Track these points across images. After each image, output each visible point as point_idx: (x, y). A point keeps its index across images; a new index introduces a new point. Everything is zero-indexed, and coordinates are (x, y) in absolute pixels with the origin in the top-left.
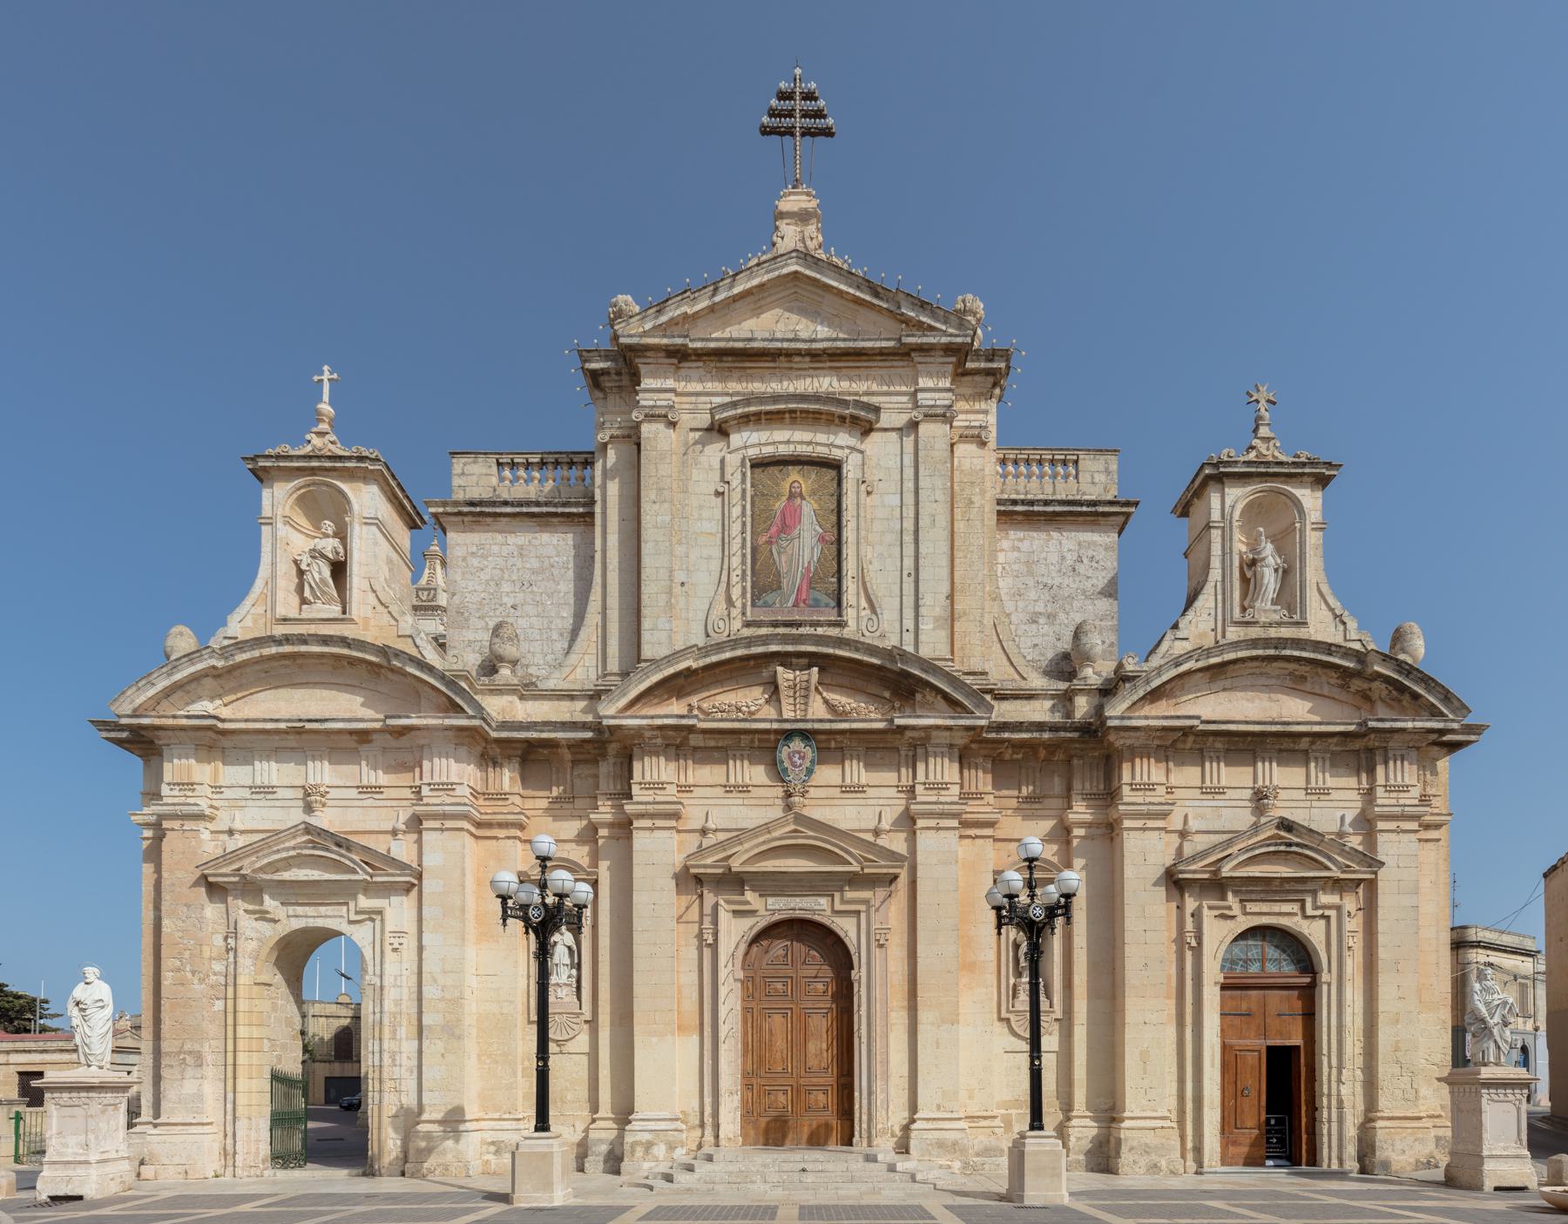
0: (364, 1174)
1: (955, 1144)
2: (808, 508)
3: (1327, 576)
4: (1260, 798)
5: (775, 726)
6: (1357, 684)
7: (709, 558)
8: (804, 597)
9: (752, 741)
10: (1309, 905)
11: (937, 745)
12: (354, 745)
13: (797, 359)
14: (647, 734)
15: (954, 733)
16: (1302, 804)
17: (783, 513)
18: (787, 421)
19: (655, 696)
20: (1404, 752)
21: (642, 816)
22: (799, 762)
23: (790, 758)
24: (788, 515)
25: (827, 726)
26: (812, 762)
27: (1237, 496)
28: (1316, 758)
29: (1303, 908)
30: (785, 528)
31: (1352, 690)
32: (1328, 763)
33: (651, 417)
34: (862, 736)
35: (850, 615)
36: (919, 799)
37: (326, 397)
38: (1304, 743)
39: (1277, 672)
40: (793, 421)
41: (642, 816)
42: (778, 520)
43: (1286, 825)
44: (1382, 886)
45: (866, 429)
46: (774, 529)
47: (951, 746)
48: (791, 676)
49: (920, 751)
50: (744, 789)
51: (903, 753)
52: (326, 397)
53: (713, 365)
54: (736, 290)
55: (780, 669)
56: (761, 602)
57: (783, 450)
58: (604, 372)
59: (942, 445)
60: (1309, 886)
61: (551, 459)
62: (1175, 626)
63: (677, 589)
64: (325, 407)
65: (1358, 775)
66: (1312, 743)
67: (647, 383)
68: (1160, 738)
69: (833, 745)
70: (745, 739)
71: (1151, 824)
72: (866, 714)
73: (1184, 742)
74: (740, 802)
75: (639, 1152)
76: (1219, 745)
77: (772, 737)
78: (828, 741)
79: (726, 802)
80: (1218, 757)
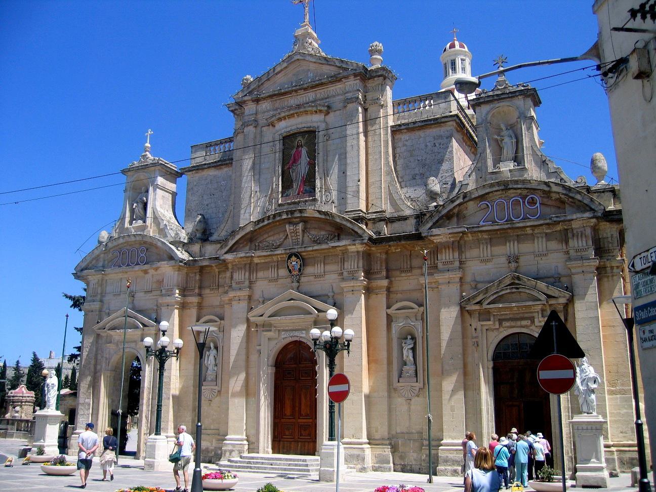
0: (135, 459)
1: (358, 456)
2: (304, 151)
8: (302, 190)
10: (536, 320)
11: (353, 252)
12: (143, 274)
13: (299, 91)
18: (296, 116)
19: (241, 244)
26: (301, 266)
28: (538, 237)
29: (533, 322)
30: (295, 161)
31: (553, 198)
32: (544, 239)
40: (298, 116)
45: (327, 113)
46: (291, 162)
47: (358, 252)
48: (292, 228)
50: (276, 280)
53: (270, 100)
55: (287, 226)
56: (285, 194)
58: (235, 110)
64: (148, 145)
73: (468, 237)
75: (228, 454)
76: (486, 237)
80: (486, 243)
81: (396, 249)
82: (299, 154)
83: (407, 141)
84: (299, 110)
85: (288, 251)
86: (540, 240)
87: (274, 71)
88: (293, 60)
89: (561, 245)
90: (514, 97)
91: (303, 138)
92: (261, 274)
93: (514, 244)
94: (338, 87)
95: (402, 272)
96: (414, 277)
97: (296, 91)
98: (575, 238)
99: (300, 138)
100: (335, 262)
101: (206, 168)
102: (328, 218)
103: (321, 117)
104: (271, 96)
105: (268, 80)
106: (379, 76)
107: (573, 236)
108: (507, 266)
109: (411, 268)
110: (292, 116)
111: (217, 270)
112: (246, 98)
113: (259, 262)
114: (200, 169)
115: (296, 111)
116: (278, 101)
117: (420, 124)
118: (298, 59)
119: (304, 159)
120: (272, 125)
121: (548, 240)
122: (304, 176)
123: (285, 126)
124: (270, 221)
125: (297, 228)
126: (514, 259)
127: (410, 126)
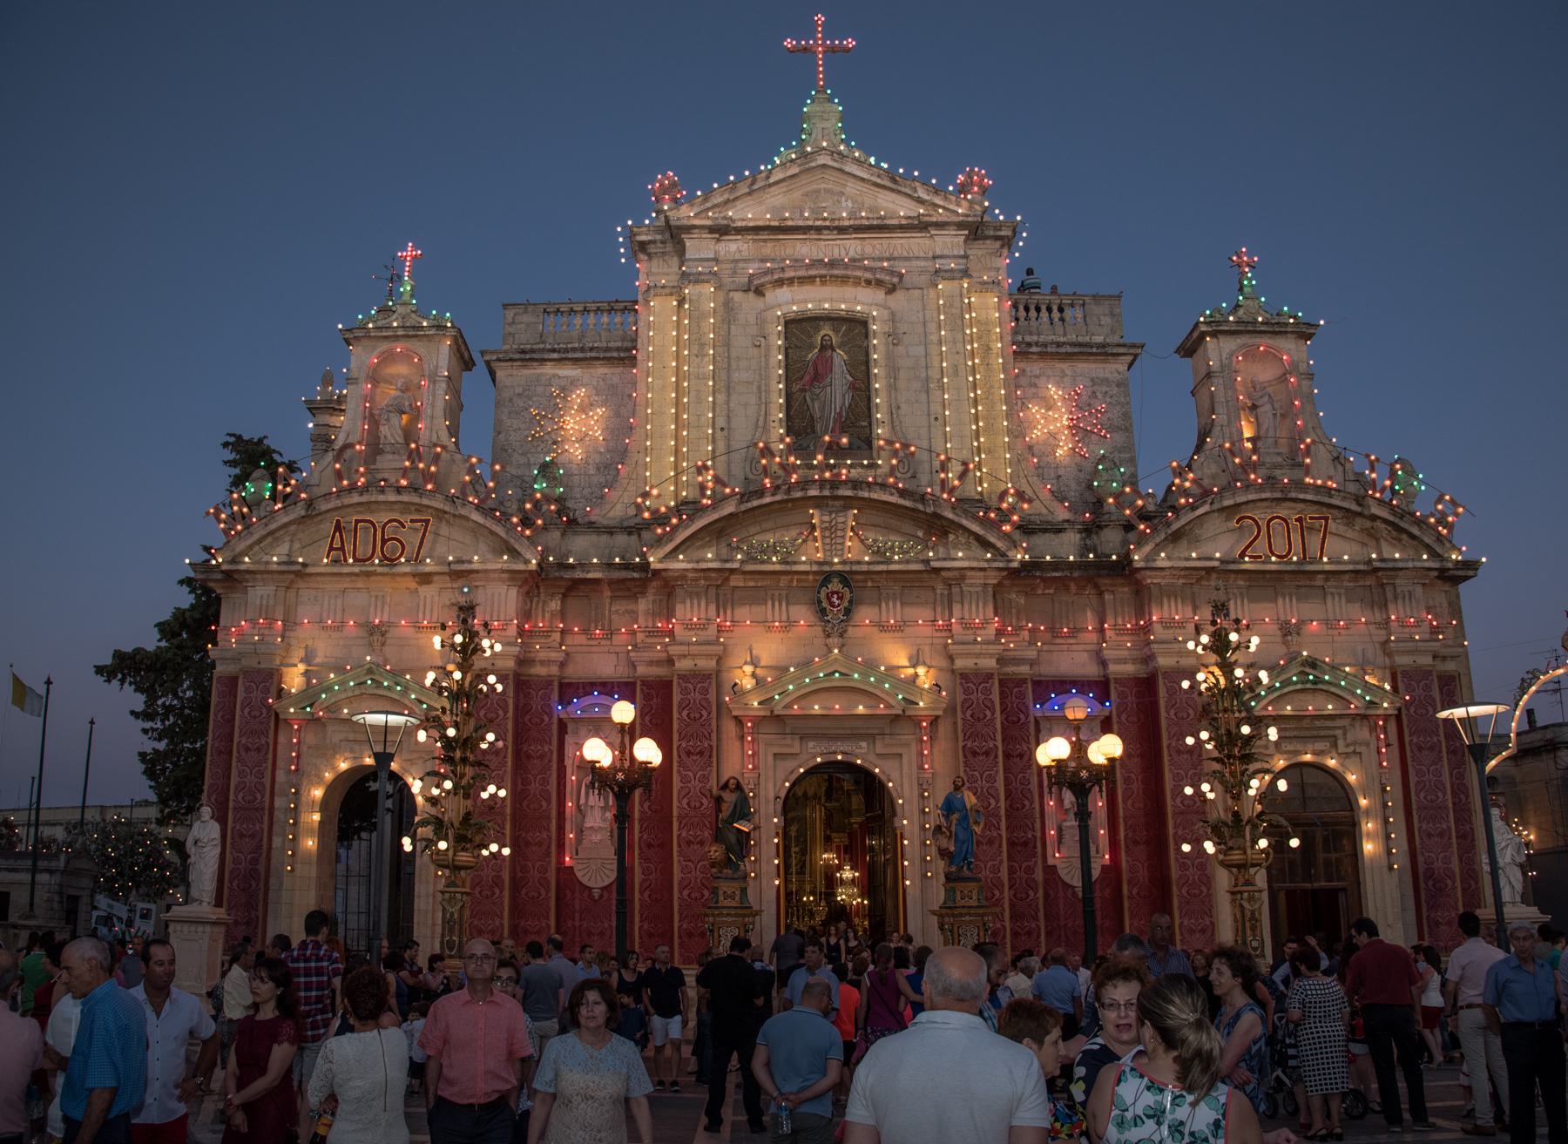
2: (839, 357)
6: (1359, 523)
7: (746, 405)
9: (791, 581)
10: (1341, 743)
11: (972, 585)
14: (690, 575)
15: (987, 573)
17: (815, 364)
20: (1411, 588)
22: (837, 602)
23: (829, 598)
24: (820, 367)
26: (851, 602)
28: (1332, 594)
29: (1335, 745)
30: (818, 377)
32: (1343, 600)
34: (898, 576)
38: (1319, 580)
40: (823, 283)
42: (810, 369)
45: (891, 290)
48: (826, 518)
49: (955, 590)
51: (939, 592)
60: (1339, 723)
61: (593, 307)
65: (1372, 608)
66: (1327, 580)
68: (1185, 577)
69: (870, 584)
70: (784, 580)
72: (902, 553)
76: (1242, 583)
77: (811, 577)
78: (866, 581)
81: (1047, 587)
83: (1036, 376)
84: (833, 273)
86: (1337, 599)
87: (768, 177)
88: (813, 164)
89: (1370, 612)
90: (1280, 333)
91: (836, 331)
92: (743, 612)
93: (1291, 600)
94: (916, 244)
96: (1081, 647)
97: (819, 229)
98: (1400, 602)
99: (826, 330)
101: (551, 360)
102: (921, 507)
103: (880, 295)
104: (757, 230)
105: (749, 194)
106: (997, 238)
107: (1396, 598)
108: (1279, 639)
110: (803, 280)
111: (609, 593)
112: (697, 222)
113: (741, 584)
114: (537, 360)
115: (823, 272)
116: (770, 245)
117: (1069, 349)
118: (824, 166)
119: (840, 377)
121: (1349, 601)
122: (840, 413)
124: (778, 498)
125: (841, 519)
126: (1287, 631)
127: (1049, 350)
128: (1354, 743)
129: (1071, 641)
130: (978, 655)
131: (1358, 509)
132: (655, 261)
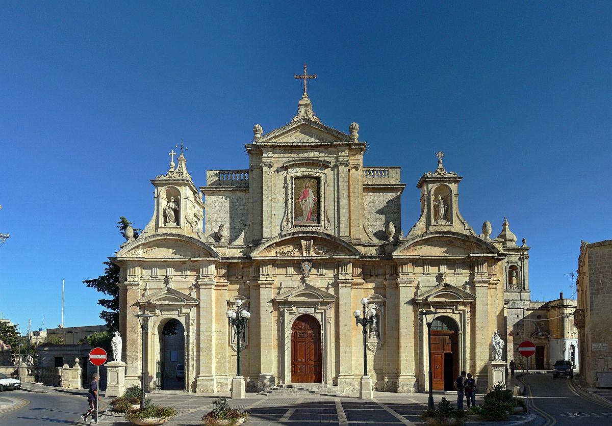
3: (459, 210)
4: (440, 278)
5: (301, 258)
6: (468, 243)
16: (453, 278)
21: (263, 284)
25: (315, 258)
26: (311, 267)
27: (433, 187)
29: (453, 311)
30: (304, 197)
33: (266, 165)
35: (322, 223)
36: (340, 278)
37: (173, 160)
39: (445, 240)
41: (263, 284)
43: (447, 286)
44: (477, 304)
46: (301, 198)
52: (173, 160)
54: (290, 128)
57: (304, 174)
59: (346, 172)
62: (415, 226)
63: (273, 215)
67: (265, 155)
71: (408, 285)
74: (289, 279)
79: (286, 279)
82: (307, 193)
85: (304, 258)
95: (372, 276)
100: (332, 267)
109: (378, 275)
119: (311, 197)
120: (285, 168)
123: (295, 172)
124: (291, 237)
128: (460, 310)
129: (376, 278)
130: (346, 283)
131: (467, 239)
132: (254, 158)
